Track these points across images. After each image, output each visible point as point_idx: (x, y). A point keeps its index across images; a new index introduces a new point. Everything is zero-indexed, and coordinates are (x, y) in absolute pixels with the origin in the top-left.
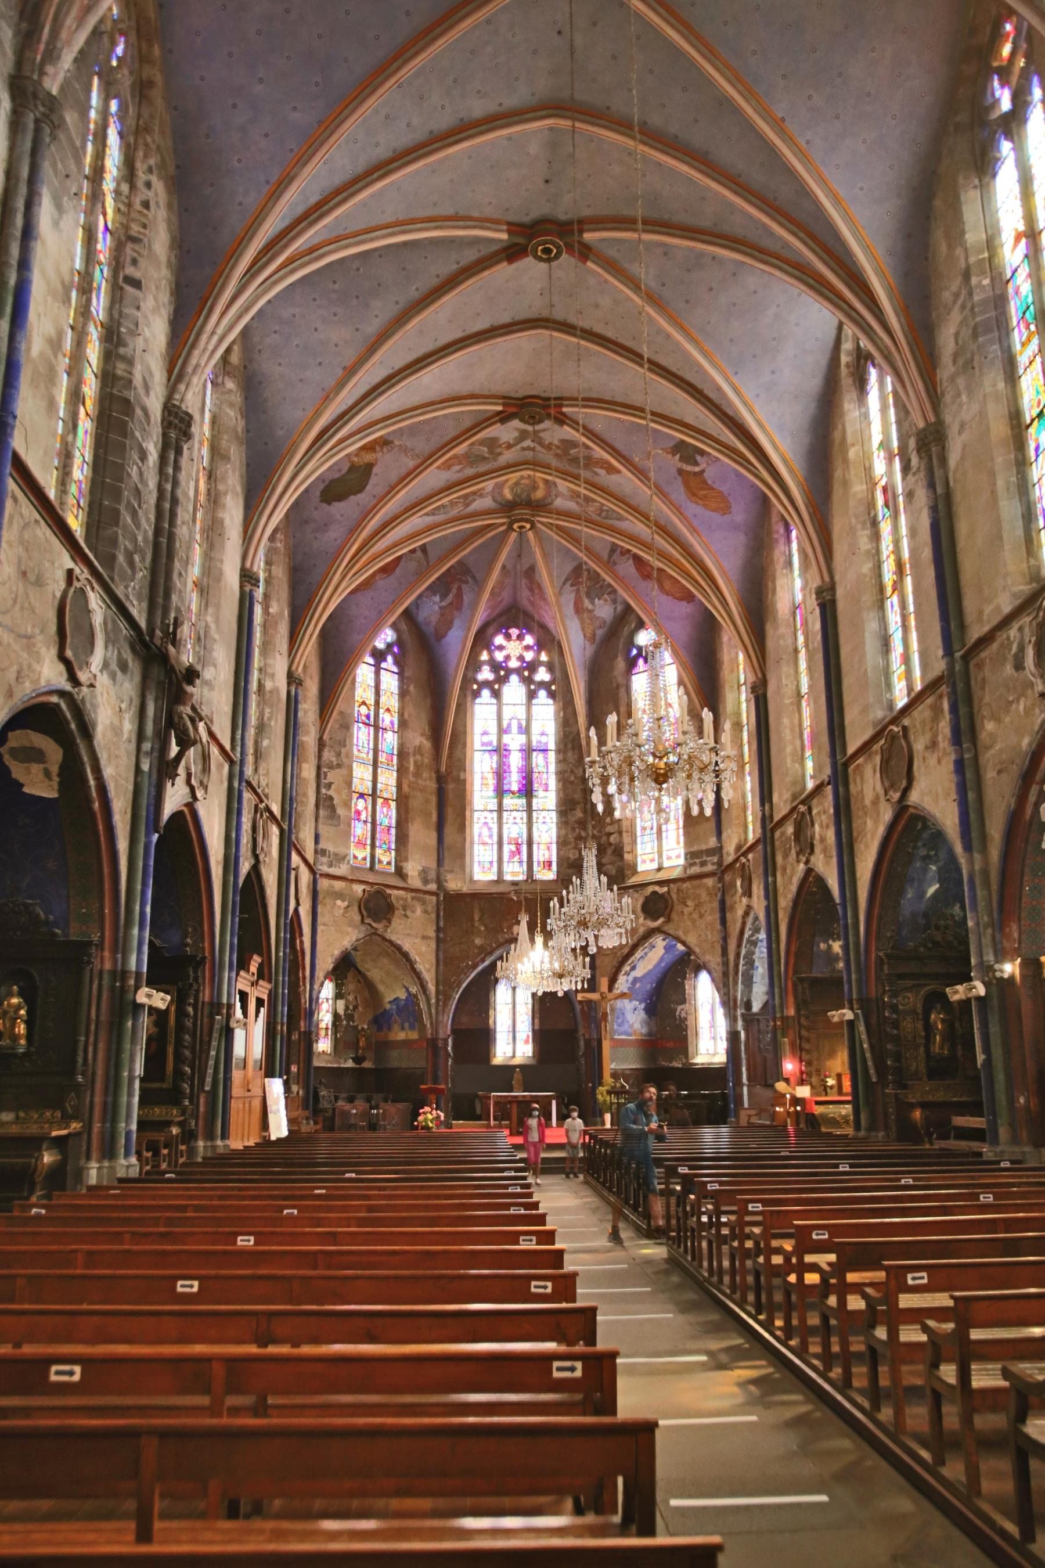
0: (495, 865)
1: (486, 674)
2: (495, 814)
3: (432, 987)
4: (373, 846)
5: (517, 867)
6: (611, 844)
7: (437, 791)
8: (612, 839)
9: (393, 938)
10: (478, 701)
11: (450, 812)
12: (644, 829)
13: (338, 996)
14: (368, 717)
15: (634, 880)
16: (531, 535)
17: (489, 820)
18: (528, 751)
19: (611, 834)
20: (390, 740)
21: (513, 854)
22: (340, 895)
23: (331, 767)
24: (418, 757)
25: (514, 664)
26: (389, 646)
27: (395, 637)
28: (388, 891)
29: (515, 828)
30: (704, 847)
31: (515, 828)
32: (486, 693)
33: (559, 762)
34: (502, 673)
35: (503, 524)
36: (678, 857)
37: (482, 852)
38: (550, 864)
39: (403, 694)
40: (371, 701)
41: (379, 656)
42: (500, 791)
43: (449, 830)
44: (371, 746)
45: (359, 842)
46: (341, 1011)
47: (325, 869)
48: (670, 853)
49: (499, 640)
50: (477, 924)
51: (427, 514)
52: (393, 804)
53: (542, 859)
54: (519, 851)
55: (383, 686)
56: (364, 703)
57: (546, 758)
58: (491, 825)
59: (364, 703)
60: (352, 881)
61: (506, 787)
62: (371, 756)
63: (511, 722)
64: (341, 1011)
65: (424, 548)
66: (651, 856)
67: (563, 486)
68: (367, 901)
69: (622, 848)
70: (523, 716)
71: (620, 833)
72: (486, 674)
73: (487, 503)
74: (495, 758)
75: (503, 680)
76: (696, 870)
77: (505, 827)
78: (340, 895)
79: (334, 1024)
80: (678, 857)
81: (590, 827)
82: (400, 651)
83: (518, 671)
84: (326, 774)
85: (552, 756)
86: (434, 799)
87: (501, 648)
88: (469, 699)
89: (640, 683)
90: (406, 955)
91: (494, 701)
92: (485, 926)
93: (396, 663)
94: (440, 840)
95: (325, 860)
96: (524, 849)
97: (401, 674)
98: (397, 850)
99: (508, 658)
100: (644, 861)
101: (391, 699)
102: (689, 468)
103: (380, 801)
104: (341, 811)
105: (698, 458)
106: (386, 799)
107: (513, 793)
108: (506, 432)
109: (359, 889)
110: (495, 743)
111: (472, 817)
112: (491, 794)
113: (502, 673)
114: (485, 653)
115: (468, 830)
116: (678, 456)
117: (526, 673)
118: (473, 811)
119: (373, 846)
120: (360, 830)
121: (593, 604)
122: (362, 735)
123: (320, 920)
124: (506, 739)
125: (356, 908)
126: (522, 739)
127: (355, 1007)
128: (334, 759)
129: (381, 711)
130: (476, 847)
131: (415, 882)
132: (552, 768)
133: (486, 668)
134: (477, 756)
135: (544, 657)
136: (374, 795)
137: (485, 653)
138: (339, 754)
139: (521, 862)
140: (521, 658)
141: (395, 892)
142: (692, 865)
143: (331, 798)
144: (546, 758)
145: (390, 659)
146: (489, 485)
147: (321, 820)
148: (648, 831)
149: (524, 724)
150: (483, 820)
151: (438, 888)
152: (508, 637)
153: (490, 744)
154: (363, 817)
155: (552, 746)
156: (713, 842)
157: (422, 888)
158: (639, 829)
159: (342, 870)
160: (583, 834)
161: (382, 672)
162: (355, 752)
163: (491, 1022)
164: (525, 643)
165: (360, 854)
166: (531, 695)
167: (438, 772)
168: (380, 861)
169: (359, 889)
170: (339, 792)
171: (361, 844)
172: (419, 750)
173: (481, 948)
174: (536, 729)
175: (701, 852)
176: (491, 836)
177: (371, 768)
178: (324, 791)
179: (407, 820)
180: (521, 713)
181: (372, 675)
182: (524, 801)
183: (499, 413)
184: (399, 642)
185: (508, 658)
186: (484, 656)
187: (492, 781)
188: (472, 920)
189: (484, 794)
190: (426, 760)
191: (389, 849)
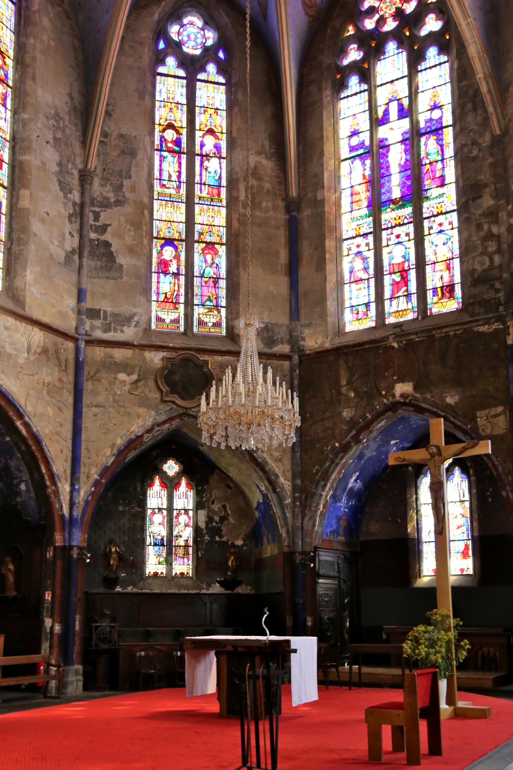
0: (373, 306)
3: (285, 483)
4: (189, 304)
5: (402, 304)
7: (285, 221)
11: (306, 249)
13: (199, 506)
14: (178, 142)
17: (363, 248)
18: (412, 139)
20: (215, 169)
21: (395, 285)
23: (106, 204)
24: (253, 182)
29: (398, 251)
32: (354, 81)
37: (355, 293)
42: (376, 206)
43: (305, 271)
45: (166, 300)
46: (202, 525)
47: (99, 334)
50: (344, 390)
52: (222, 250)
53: (439, 284)
54: (405, 281)
56: (170, 126)
57: (440, 141)
59: (170, 126)
60: (142, 347)
64: (202, 525)
68: (172, 372)
72: (354, 55)
78: (125, 367)
79: (195, 541)
81: (503, 215)
83: (396, 35)
85: (448, 135)
86: (282, 235)
88: (327, 93)
92: (356, 391)
93: (220, 71)
95: (98, 323)
96: (412, 275)
97: (231, 88)
104: (123, 260)
107: (394, 202)
110: (367, 143)
111: (339, 249)
112: (365, 211)
113: (373, 45)
114: (351, 28)
115: (330, 267)
118: (340, 240)
119: (189, 304)
123: (87, 399)
125: (151, 383)
126: (405, 124)
127: (223, 519)
129: (198, 134)
136: (189, 240)
139: (408, 296)
143: (107, 244)
144: (440, 141)
147: (85, 271)
149: (406, 102)
150: (355, 250)
151: (292, 350)
153: (362, 145)
154: (173, 268)
155: (448, 119)
160: (495, 230)
163: (410, 528)
165: (168, 316)
166: (415, 60)
167: (286, 198)
170: (120, 236)
171: (170, 301)
172: (255, 173)
173: (352, 423)
174: (423, 102)
176: (366, 269)
177: (183, 207)
179: (237, 266)
180: (402, 89)
188: (337, 384)
190: (267, 186)
191: (217, 307)
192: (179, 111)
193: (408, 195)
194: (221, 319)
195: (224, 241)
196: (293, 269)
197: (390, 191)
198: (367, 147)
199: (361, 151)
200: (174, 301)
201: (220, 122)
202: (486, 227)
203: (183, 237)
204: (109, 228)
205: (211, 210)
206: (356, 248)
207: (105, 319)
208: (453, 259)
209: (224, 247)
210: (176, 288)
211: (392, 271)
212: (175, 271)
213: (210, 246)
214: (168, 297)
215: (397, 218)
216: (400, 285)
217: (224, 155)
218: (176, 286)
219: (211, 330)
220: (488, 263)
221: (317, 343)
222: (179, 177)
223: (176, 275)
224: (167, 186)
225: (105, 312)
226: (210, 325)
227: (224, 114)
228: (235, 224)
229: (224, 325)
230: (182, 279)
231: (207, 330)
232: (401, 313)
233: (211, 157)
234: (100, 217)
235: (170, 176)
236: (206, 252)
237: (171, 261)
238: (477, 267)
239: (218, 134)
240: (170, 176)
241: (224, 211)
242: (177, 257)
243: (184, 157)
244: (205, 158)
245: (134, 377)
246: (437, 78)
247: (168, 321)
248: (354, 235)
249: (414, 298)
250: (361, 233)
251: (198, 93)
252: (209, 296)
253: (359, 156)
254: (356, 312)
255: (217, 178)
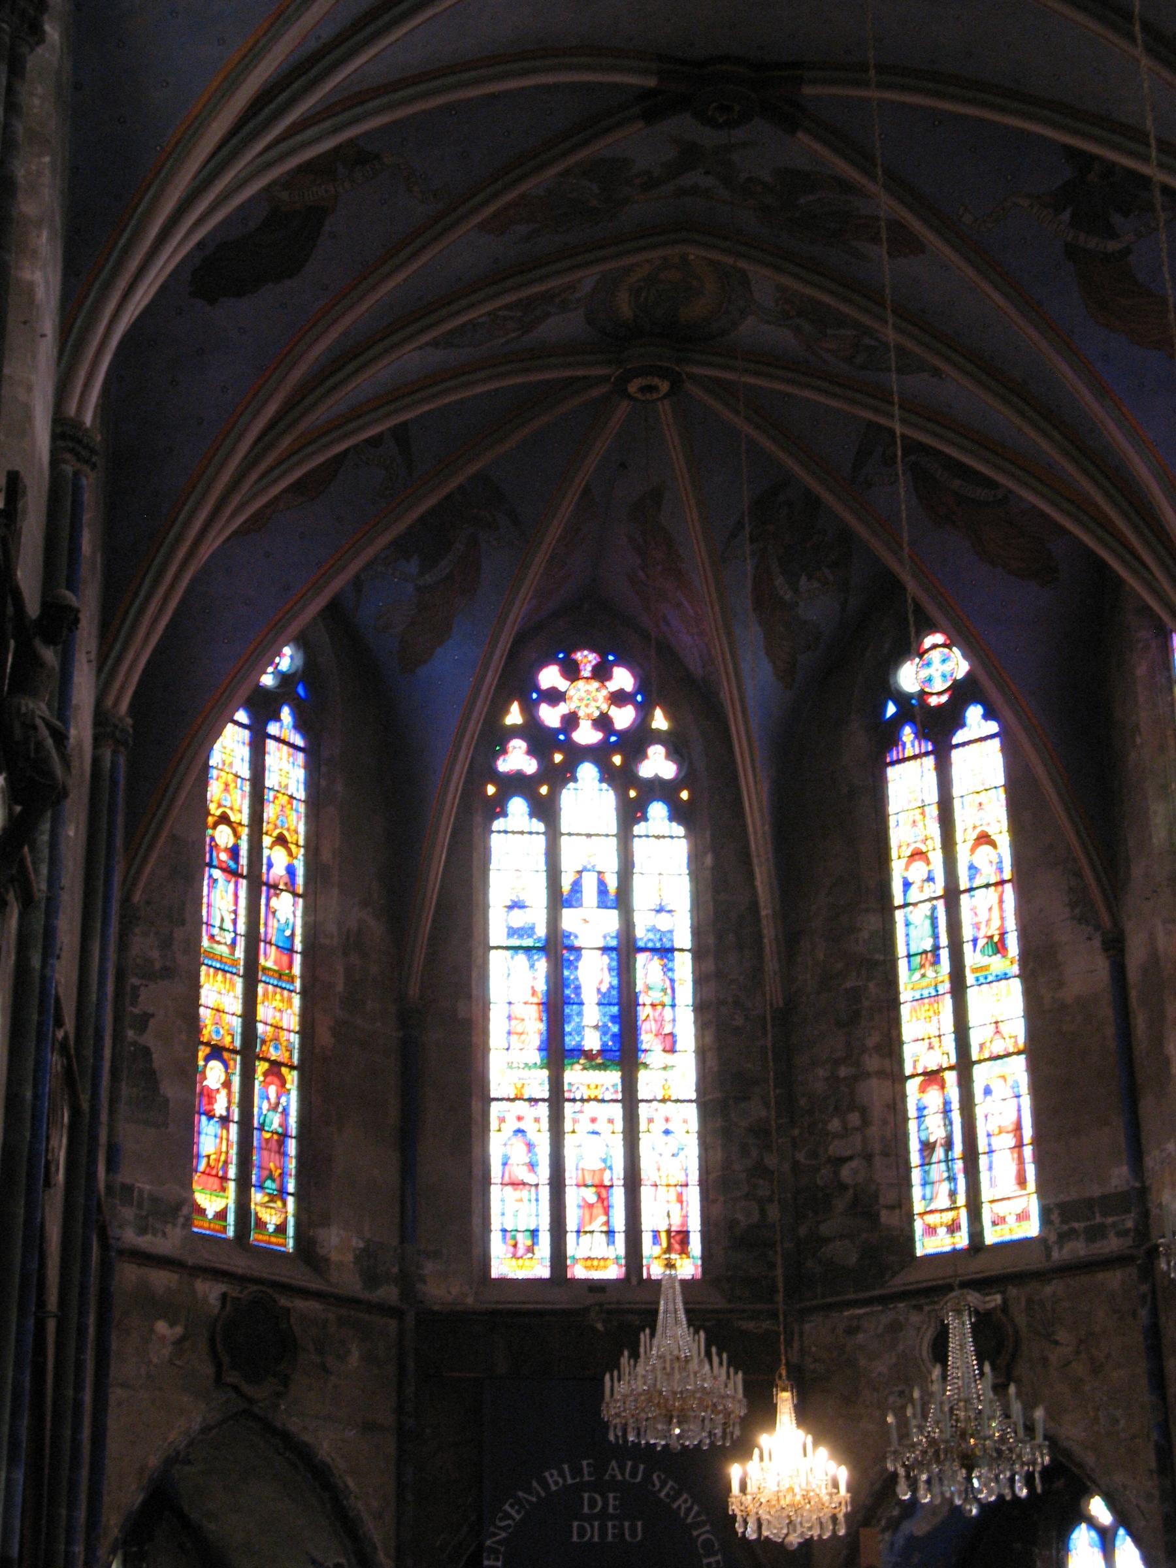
0: (545, 1238)
1: (517, 759)
2: (543, 1110)
6: (843, 1187)
8: (845, 1172)
9: (293, 1425)
10: (498, 824)
12: (927, 1147)
14: (234, 852)
15: (898, 1283)
16: (665, 409)
18: (625, 951)
19: (843, 1160)
22: (165, 1308)
23: (149, 975)
25: (586, 735)
26: (285, 679)
27: (299, 662)
28: (283, 1301)
30: (1096, 1191)
31: (594, 1145)
32: (518, 806)
33: (700, 980)
34: (558, 758)
35: (606, 379)
36: (1022, 1217)
37: (510, 1207)
38: (682, 1237)
39: (317, 800)
40: (242, 816)
41: (264, 709)
42: (557, 1052)
44: (242, 928)
48: (1001, 1209)
49: (550, 677)
51: (435, 343)
55: (271, 780)
56: (224, 819)
57: (667, 969)
58: (532, 1135)
59: (224, 819)
61: (570, 1042)
62: (240, 953)
63: (588, 877)
65: (401, 434)
66: (948, 1217)
67: (765, 283)
69: (876, 1196)
70: (610, 865)
71: (869, 1158)
72: (517, 759)
73: (561, 326)
74: (542, 965)
75: (561, 776)
76: (1078, 1249)
77: (569, 1141)
78: (165, 1308)
80: (1022, 1217)
82: (310, 697)
84: (135, 989)
85: (684, 965)
87: (554, 697)
88: (478, 819)
89: (908, 784)
90: (320, 1476)
91: (540, 826)
93: (298, 726)
94: (408, 1170)
95: (128, 1213)
96: (618, 1197)
98: (299, 1196)
99: (571, 721)
100: (931, 1230)
101: (289, 815)
102: (1093, 243)
103: (262, 1067)
104: (170, 1089)
105: (1117, 219)
106: (275, 1066)
107: (589, 1055)
108: (640, 146)
109: (211, 1292)
110: (541, 931)
112: (536, 1057)
113: (558, 756)
114: (515, 708)
116: (1066, 216)
117: (617, 760)
118: (487, 1100)
120: (213, 1141)
121: (796, 591)
122: (222, 901)
123: (116, 1371)
124: (570, 919)
126: (611, 920)
128: (155, 954)
129: (267, 841)
130: (495, 1192)
131: (349, 1282)
132: (685, 993)
133: (518, 746)
134: (498, 963)
135: (660, 721)
137: (515, 708)
138: (166, 944)
139: (610, 1233)
140: (603, 722)
141: (300, 1304)
142: (1063, 1237)
143: (146, 1052)
145: (286, 713)
146: (588, 279)
148: (939, 1153)
149: (612, 884)
150: (511, 1125)
152: (571, 672)
153: (529, 931)
154: (220, 1108)
155: (683, 938)
156: (1119, 1177)
157: (366, 1295)
158: (914, 1146)
159: (166, 1243)
161: (271, 745)
162: (205, 943)
164: (612, 686)
166: (630, 815)
168: (260, 1224)
169: (211, 1292)
175: (1090, 1203)
176: (532, 1166)
177: (239, 983)
178: (130, 1034)
181: (246, 752)
182: (613, 1077)
183: (646, 94)
184: (308, 673)
185: (571, 721)
186: (514, 716)
187: (534, 1028)
189: (515, 1056)
191: (282, 1193)
192: (239, 792)
193: (611, 1050)
194: (286, 1218)
195: (295, 1061)
196: (407, 1138)
197: (579, 1030)
198: (539, 940)
199: (529, 942)
200: (220, 1174)
201: (296, 824)
202: (754, 1153)
203: (238, 1044)
204: (152, 1023)
205: (278, 997)
206: (515, 1120)
207: (140, 1206)
208: (687, 1185)
209: (295, 1073)
210: (224, 1149)
211: (581, 1182)
212: (224, 1113)
213: (275, 1067)
214: (212, 1163)
215: (592, 1086)
216: (595, 1211)
217: (300, 890)
218: (224, 1142)
219: (273, 1240)
220: (756, 1217)
221: (449, 1293)
222: (235, 922)
223: (225, 1121)
224: (217, 938)
225: (141, 1191)
226: (271, 1228)
227: (302, 808)
228: (325, 1037)
229: (291, 1231)
230: (234, 1128)
231: (266, 1238)
232: (595, 1263)
233: (282, 890)
234: (138, 996)
235: (222, 920)
236: (269, 1079)
237: (218, 1090)
238: (740, 1216)
239: (293, 847)
240: (222, 920)
241: (296, 1000)
242: (227, 1084)
243: (243, 883)
244: (272, 891)
245: (179, 1330)
246: (666, 860)
247: (210, 1214)
248: (512, 1096)
249: (620, 1239)
250: (526, 1097)
251: (269, 760)
252: (271, 1171)
253: (527, 949)
254: (511, 1242)
255: (288, 933)
